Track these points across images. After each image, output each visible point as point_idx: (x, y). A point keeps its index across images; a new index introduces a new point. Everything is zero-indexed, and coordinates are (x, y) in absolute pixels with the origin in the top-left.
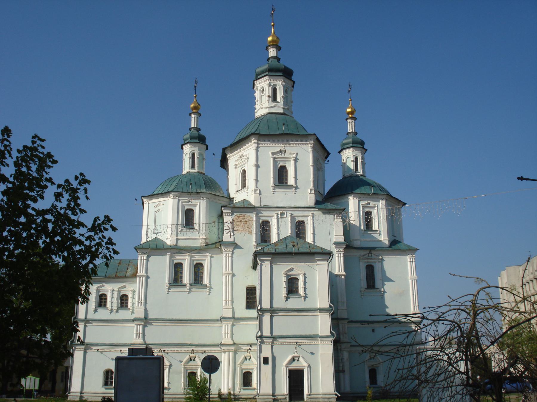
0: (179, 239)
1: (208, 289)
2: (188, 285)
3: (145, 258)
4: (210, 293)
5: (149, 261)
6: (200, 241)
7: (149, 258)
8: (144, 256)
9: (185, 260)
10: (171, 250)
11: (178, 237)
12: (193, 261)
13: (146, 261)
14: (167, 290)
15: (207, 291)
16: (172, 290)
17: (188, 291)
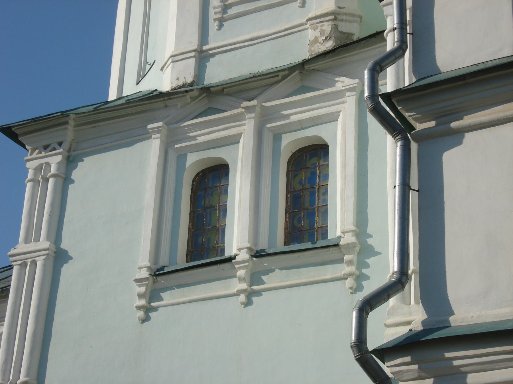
0: (213, 55)
1: (346, 258)
2: (244, 256)
3: (53, 170)
4: (364, 283)
5: (72, 182)
6: (311, 34)
7: (76, 167)
8: (48, 164)
9: (234, 140)
10: (166, 106)
11: (205, 48)
12: (277, 138)
13: (55, 185)
14: (143, 302)
15: (345, 269)
16: (168, 297)
17: (244, 286)
